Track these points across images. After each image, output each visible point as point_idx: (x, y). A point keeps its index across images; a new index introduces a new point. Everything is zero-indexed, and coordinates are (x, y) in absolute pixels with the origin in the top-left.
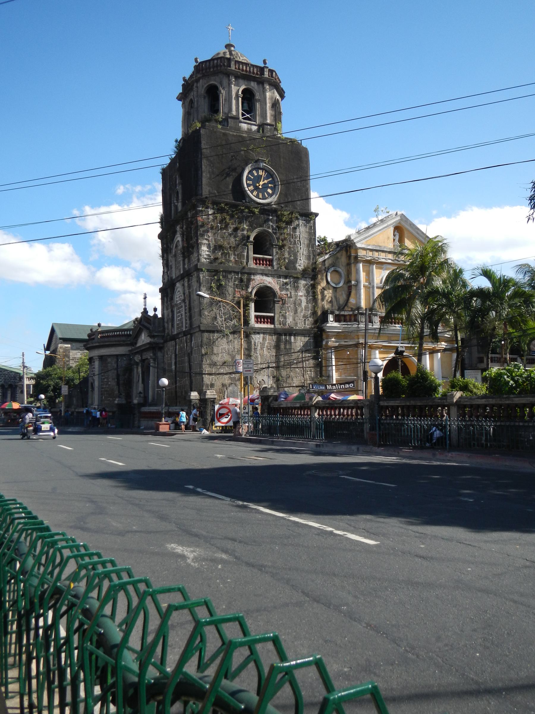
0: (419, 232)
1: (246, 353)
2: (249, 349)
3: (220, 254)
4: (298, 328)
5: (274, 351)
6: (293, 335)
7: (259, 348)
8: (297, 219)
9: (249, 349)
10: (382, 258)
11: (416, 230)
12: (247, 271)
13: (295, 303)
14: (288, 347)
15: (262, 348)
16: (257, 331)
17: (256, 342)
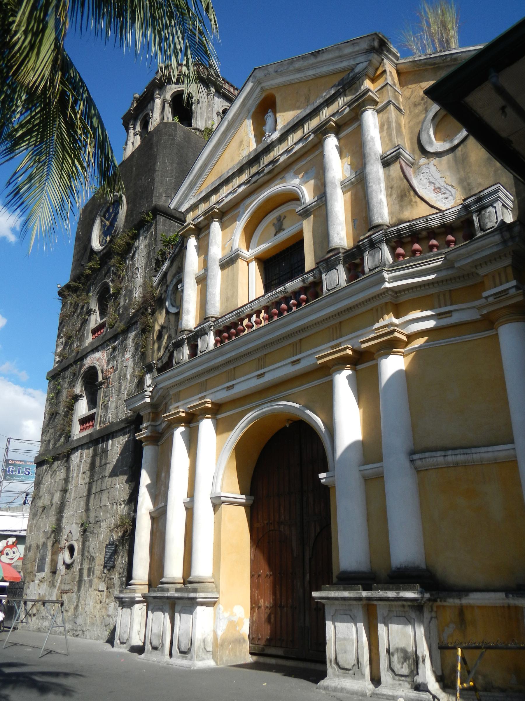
0: (297, 65)
1: (64, 486)
2: (66, 480)
3: (68, 348)
4: (118, 420)
5: (88, 473)
6: (111, 436)
7: (75, 475)
8: (135, 237)
9: (66, 480)
10: (226, 197)
11: (291, 68)
12: (79, 357)
13: (119, 378)
14: (103, 463)
15: (78, 475)
16: (75, 446)
17: (74, 464)
